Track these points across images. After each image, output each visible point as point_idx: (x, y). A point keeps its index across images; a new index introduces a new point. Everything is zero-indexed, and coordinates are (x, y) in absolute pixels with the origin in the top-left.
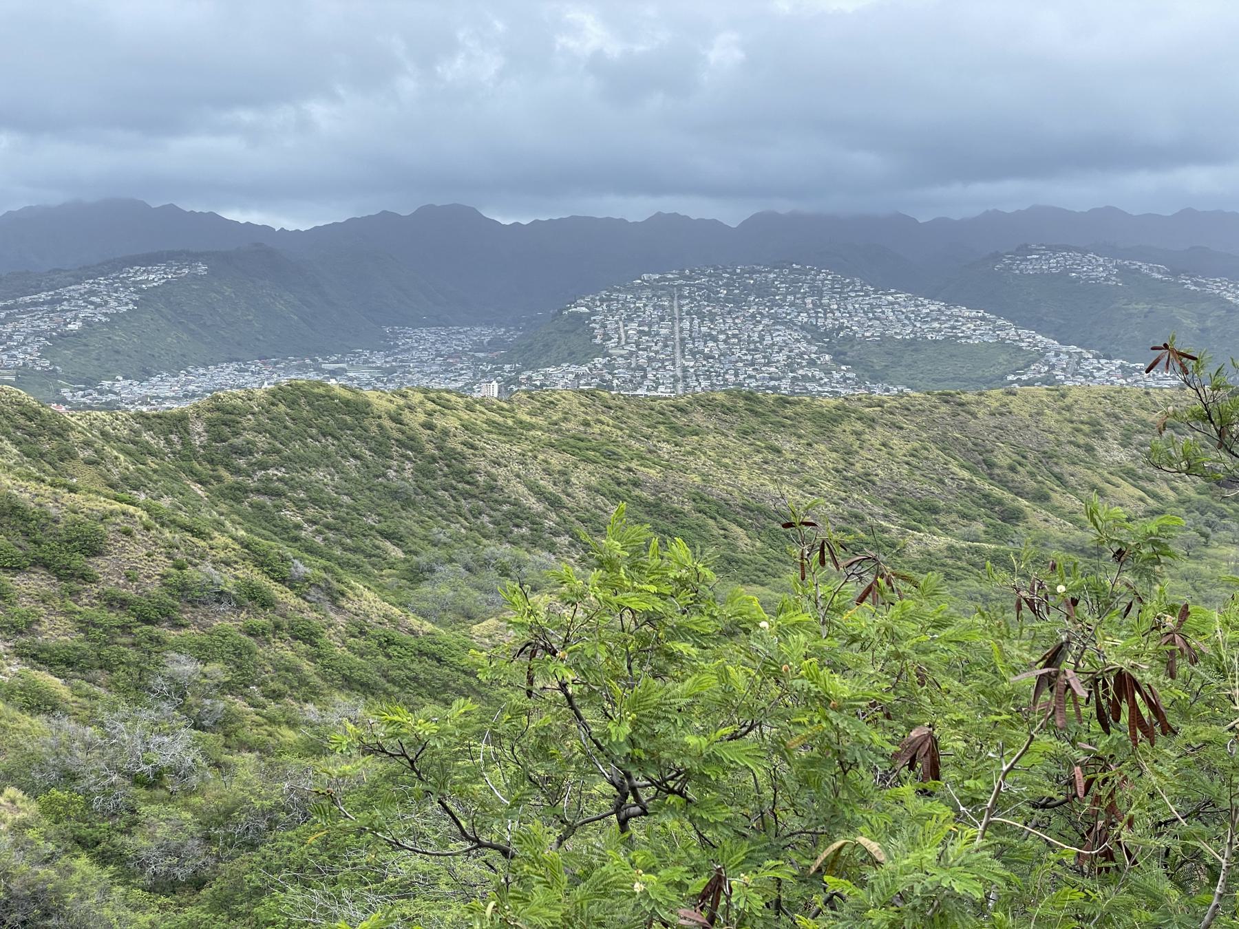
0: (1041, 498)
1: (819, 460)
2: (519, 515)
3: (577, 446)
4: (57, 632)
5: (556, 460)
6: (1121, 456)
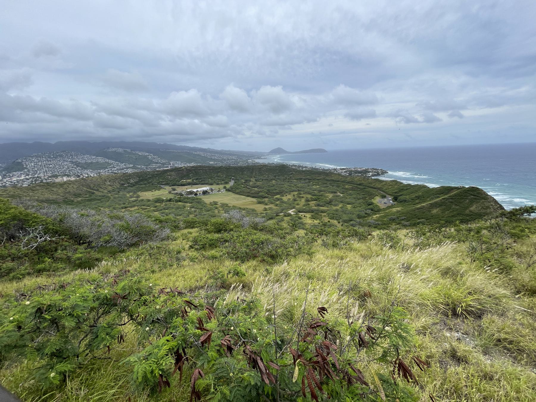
0: (98, 190)
1: (61, 190)
6: (109, 183)
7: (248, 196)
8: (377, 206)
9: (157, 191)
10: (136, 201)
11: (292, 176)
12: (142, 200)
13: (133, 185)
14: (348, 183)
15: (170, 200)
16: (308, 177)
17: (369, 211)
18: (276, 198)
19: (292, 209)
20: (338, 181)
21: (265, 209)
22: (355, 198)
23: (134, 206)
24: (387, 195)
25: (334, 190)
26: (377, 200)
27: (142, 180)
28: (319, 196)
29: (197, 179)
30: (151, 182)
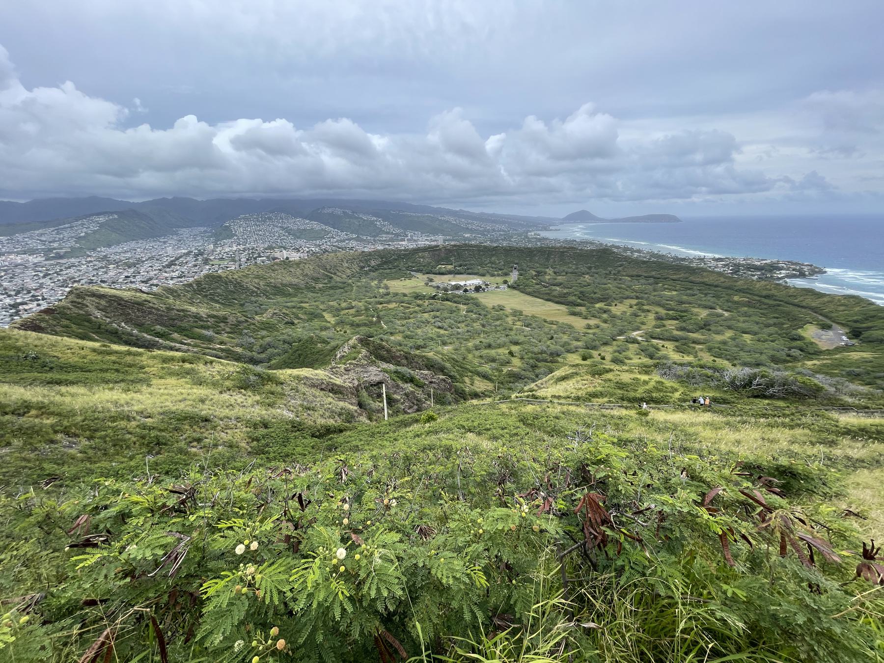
0: (335, 274)
2: (253, 292)
3: (258, 277)
4: (228, 330)
5: (256, 281)
7: (548, 300)
8: (812, 343)
9: (408, 281)
10: (388, 294)
11: (620, 268)
12: (396, 294)
13: (374, 269)
14: (740, 291)
15: (433, 298)
16: (653, 273)
17: (796, 353)
18: (600, 309)
19: (634, 330)
20: (716, 286)
21: (589, 327)
22: (757, 323)
23: (389, 302)
24: (834, 324)
25: (710, 304)
26: (810, 332)
27: (385, 263)
28: (681, 311)
29: (460, 266)
30: (398, 266)
